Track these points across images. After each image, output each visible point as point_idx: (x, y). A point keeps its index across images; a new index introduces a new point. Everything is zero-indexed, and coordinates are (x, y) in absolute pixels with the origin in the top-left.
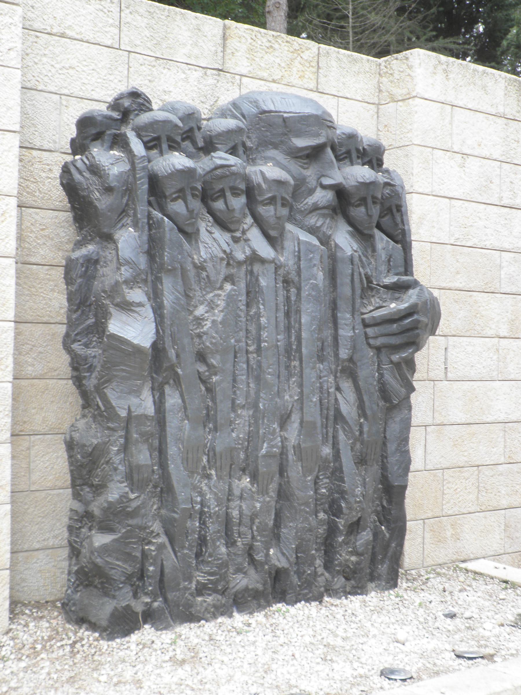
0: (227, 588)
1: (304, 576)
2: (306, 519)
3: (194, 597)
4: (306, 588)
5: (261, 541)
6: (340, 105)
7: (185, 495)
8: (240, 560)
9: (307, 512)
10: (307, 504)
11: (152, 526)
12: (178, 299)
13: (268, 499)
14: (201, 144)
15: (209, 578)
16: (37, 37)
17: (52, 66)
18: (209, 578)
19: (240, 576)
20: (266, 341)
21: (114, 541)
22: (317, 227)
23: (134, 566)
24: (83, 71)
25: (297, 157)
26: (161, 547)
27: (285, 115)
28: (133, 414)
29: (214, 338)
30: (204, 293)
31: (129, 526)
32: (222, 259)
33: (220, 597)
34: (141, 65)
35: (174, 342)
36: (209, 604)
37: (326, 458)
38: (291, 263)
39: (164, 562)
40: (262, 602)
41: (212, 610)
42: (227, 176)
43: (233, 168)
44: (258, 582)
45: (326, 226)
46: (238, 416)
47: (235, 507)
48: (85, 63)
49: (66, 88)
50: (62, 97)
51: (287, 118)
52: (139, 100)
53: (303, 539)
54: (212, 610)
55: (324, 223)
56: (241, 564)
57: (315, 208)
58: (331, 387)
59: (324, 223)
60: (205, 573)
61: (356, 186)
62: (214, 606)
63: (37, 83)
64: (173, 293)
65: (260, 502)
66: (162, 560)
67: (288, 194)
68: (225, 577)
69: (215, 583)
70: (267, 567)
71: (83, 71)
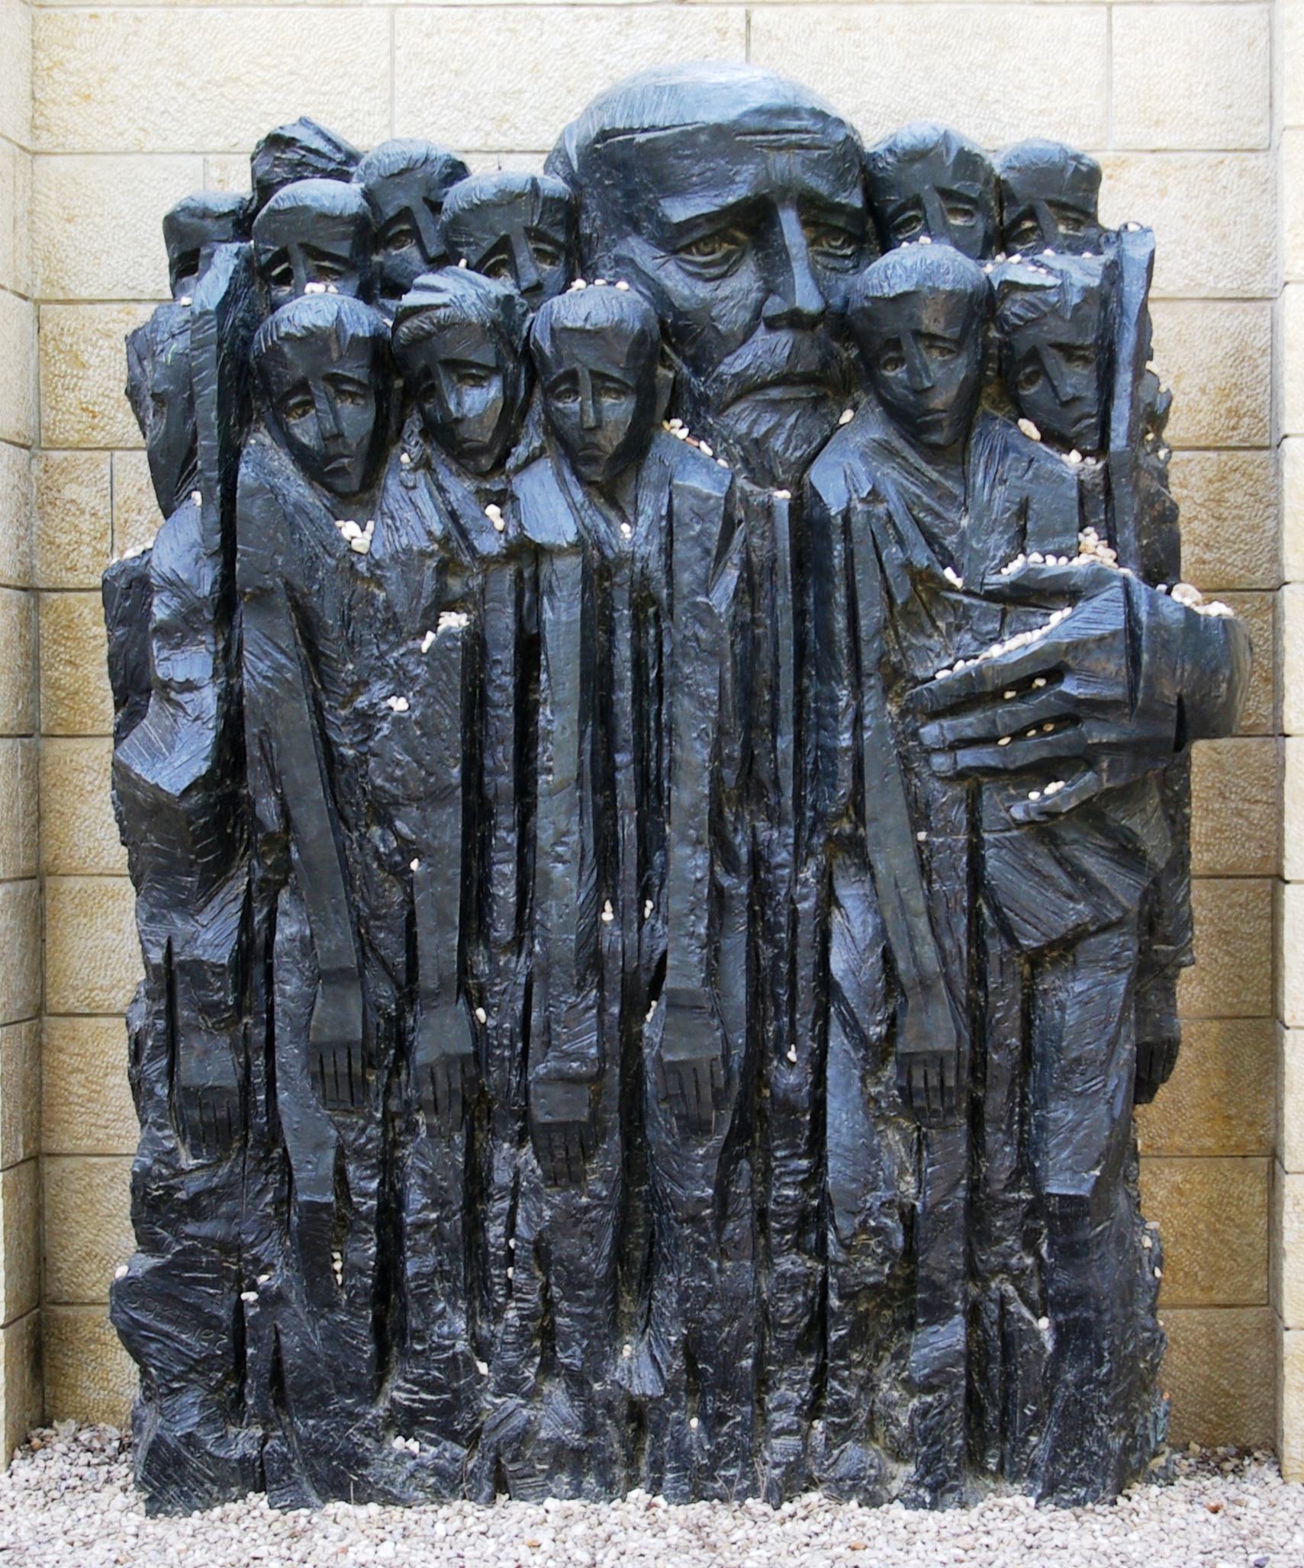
0: (479, 1431)
1: (725, 1429)
2: (703, 1266)
3: (379, 1440)
4: (728, 1465)
5: (569, 1315)
6: (1116, 30)
7: (315, 1169)
8: (510, 1357)
9: (700, 1246)
10: (694, 1220)
11: (252, 1245)
12: (279, 668)
13: (584, 1200)
14: (433, 251)
15: (424, 1396)
16: (138, 20)
17: (179, 84)
18: (424, 1396)
19: (512, 1402)
20: (549, 771)
21: (155, 1271)
22: (756, 441)
23: (213, 1342)
24: (265, 82)
25: (687, 249)
26: (271, 1300)
27: (640, 138)
28: (176, 959)
29: (398, 764)
30: (384, 647)
31: (188, 1237)
32: (423, 554)
33: (461, 1452)
34: (429, 35)
35: (275, 777)
36: (421, 1466)
37: (787, 1100)
38: (653, 548)
39: (283, 1339)
40: (590, 1481)
41: (432, 1481)
42: (430, 334)
43: (441, 313)
44: (566, 1425)
45: (783, 437)
46: (498, 972)
47: (497, 1217)
48: (267, 60)
49: (218, 133)
50: (210, 158)
51: (641, 145)
52: (289, 155)
53: (701, 1321)
54: (432, 1481)
55: (779, 425)
56: (512, 1369)
57: (748, 387)
58: (805, 898)
59: (779, 425)
60: (413, 1382)
61: (863, 309)
62: (438, 1471)
63: (141, 135)
64: (265, 653)
65: (552, 1207)
66: (277, 1333)
67: (616, 364)
68: (469, 1401)
69: (447, 1411)
70: (597, 1387)
71: (265, 82)
